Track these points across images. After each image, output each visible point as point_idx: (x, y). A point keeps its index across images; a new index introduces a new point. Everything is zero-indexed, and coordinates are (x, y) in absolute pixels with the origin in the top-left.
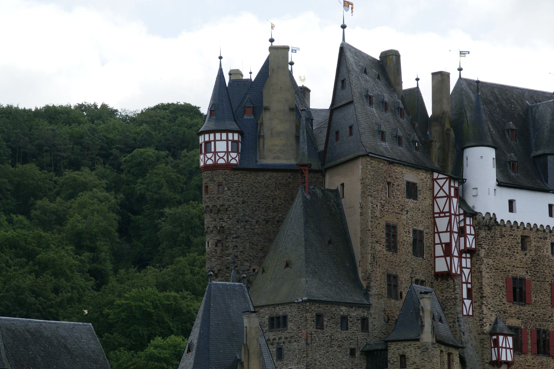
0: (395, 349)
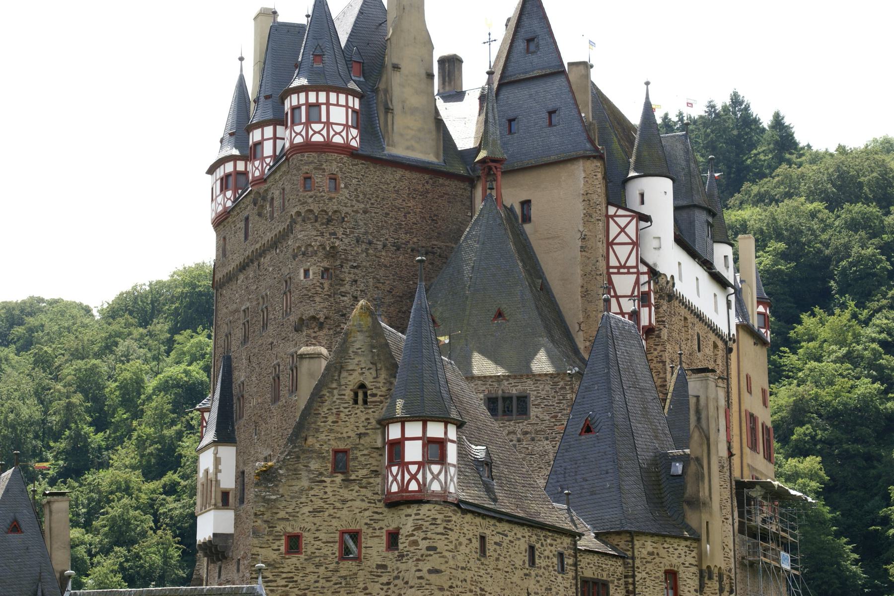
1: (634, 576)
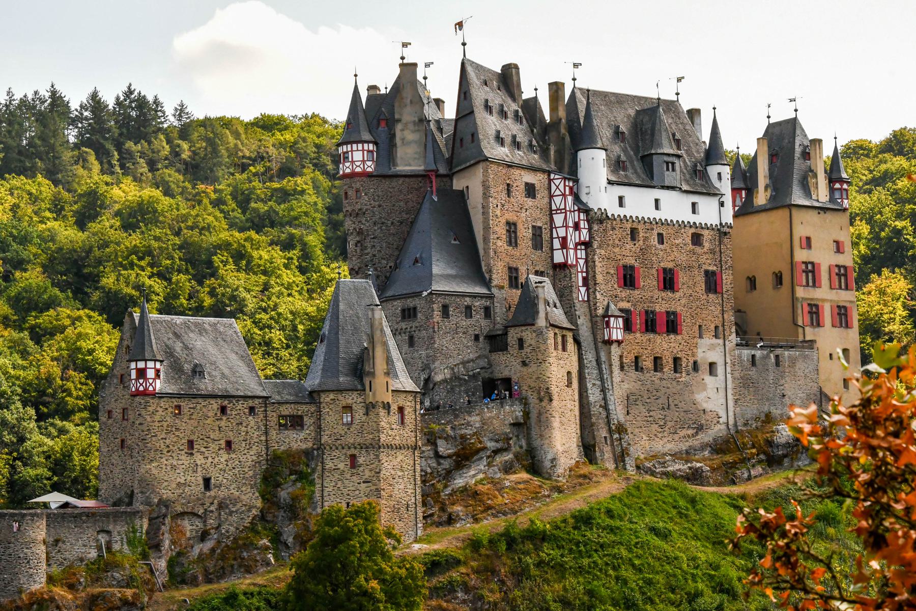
1: (320, 411)
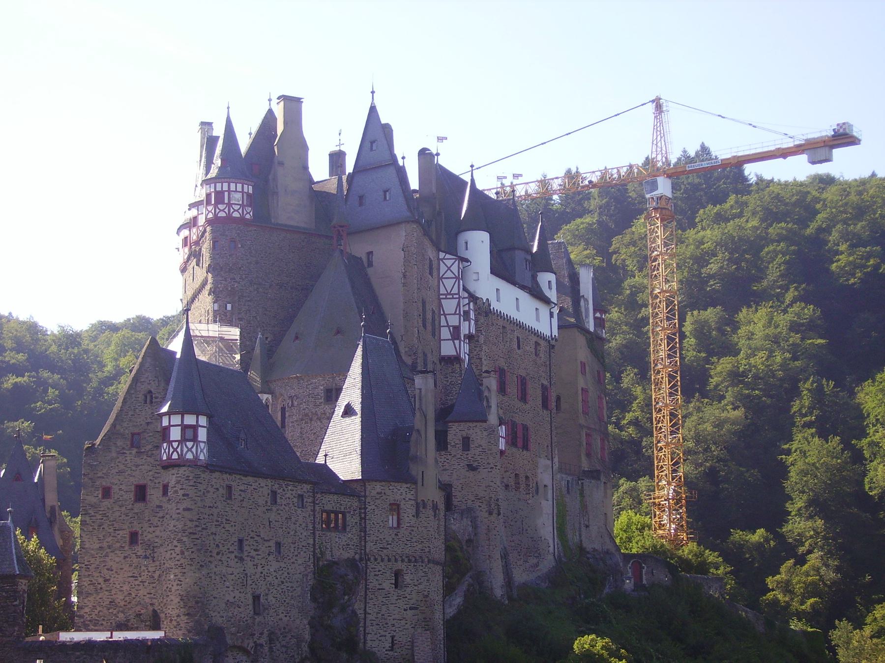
0: (457, 431)
1: (365, 508)
